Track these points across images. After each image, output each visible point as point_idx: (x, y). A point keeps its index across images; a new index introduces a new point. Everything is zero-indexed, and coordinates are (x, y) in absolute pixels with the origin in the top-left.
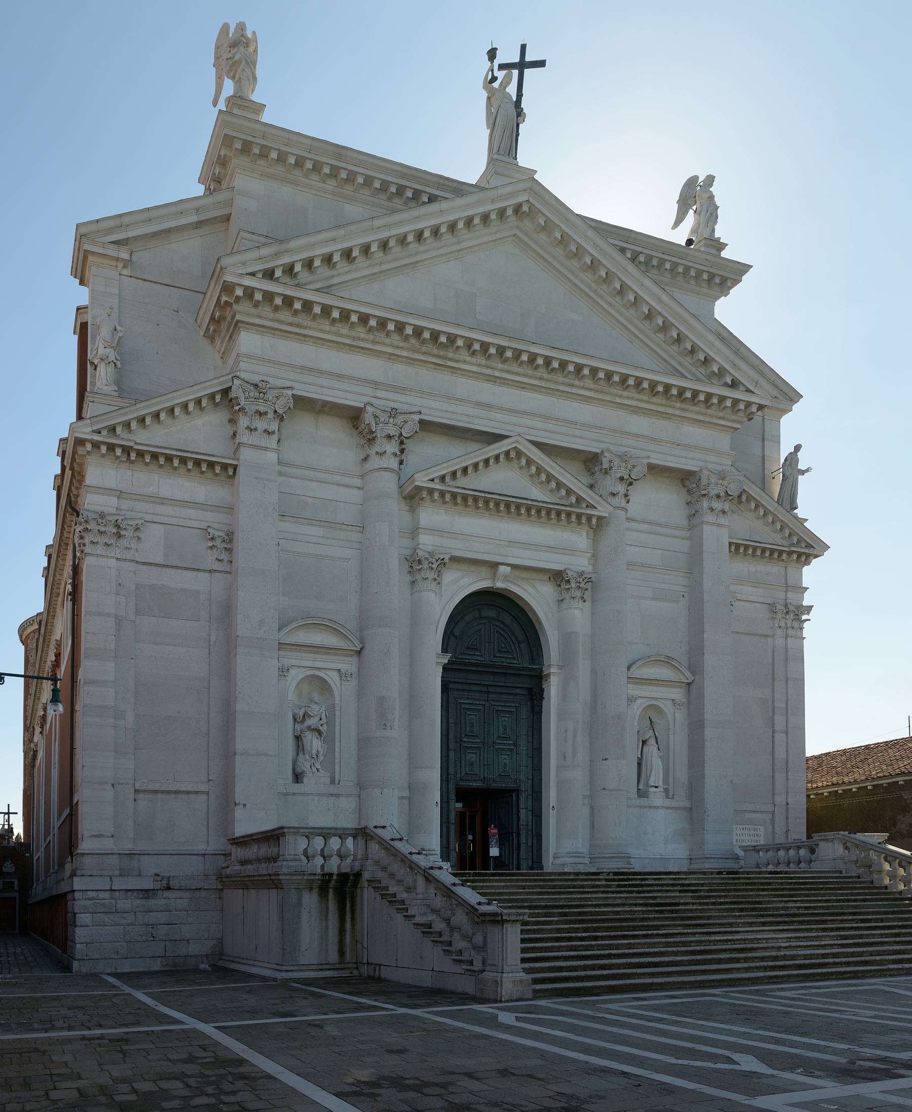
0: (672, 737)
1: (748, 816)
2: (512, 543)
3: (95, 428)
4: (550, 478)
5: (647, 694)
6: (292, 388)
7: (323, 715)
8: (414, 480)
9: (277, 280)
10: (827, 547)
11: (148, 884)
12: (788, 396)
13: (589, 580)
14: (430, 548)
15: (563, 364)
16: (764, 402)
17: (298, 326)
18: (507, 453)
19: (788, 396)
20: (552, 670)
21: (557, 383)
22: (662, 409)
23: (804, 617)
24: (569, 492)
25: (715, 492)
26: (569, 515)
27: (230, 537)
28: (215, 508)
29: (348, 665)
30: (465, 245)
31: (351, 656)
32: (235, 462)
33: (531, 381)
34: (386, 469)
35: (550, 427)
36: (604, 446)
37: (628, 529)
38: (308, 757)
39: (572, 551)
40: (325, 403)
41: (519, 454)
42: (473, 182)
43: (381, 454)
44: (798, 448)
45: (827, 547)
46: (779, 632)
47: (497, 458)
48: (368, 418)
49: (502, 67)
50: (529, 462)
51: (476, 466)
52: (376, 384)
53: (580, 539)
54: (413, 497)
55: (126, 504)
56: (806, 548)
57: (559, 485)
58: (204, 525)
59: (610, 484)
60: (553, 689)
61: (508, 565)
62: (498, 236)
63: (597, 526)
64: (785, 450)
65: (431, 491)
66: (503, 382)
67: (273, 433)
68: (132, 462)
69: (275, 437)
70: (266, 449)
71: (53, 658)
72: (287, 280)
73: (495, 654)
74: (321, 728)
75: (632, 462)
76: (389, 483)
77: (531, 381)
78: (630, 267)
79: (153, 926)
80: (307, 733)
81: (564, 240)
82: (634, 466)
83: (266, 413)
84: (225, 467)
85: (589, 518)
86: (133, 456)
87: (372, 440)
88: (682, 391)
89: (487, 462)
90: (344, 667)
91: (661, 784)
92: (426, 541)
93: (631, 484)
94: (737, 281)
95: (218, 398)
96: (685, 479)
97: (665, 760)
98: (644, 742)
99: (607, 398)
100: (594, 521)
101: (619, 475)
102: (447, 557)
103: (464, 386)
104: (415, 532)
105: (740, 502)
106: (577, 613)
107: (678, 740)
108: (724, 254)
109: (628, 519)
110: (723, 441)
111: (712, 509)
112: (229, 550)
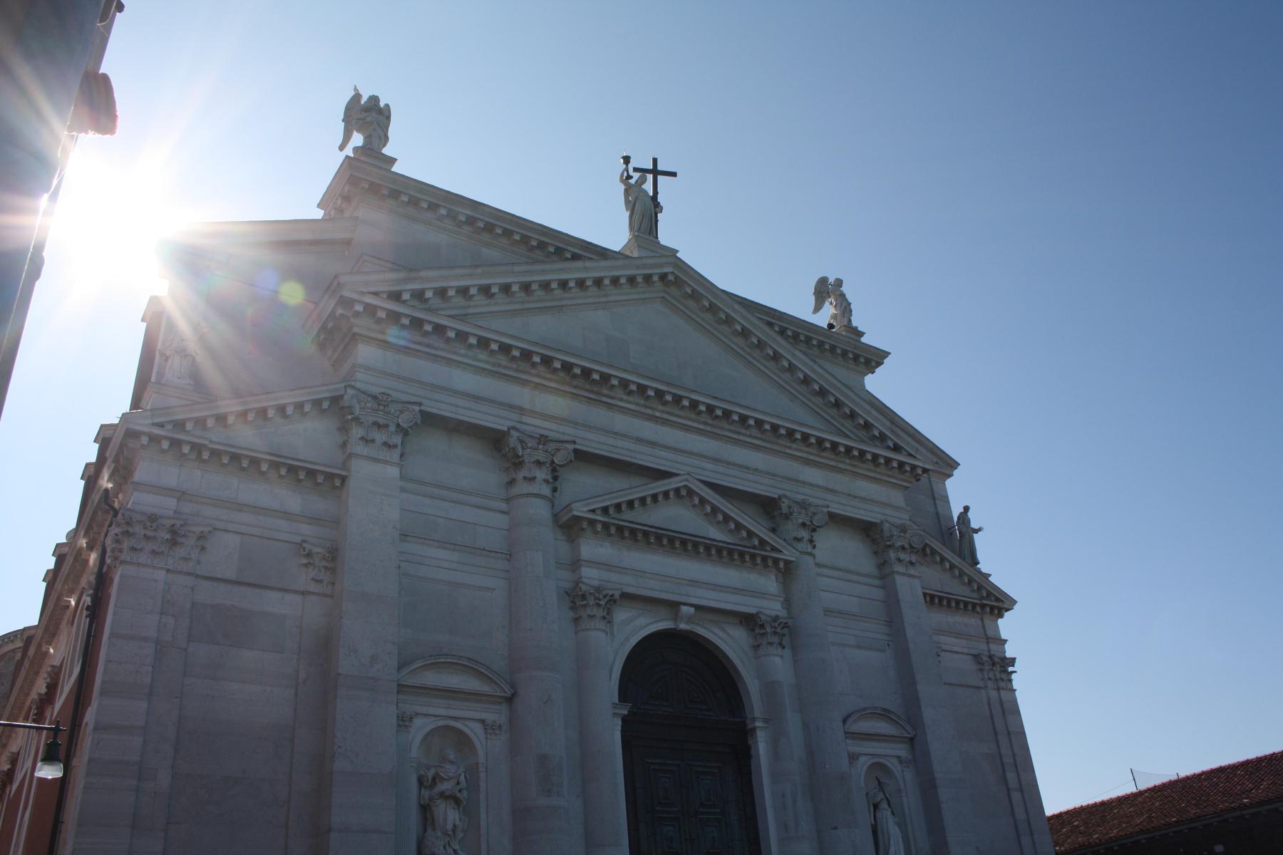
0: (905, 799)
2: (694, 583)
3: (156, 420)
4: (727, 518)
6: (420, 404)
7: (462, 777)
8: (571, 510)
9: (404, 302)
10: (1015, 602)
12: (947, 465)
13: (786, 626)
14: (596, 583)
15: (727, 414)
16: (927, 466)
17: (429, 346)
18: (677, 490)
19: (947, 465)
20: (757, 724)
21: (723, 429)
22: (832, 463)
23: (1010, 669)
24: (751, 534)
25: (899, 544)
26: (753, 556)
27: (334, 554)
28: (315, 520)
30: (611, 299)
31: (500, 703)
32: (344, 473)
33: (695, 425)
34: (537, 496)
35: (721, 469)
36: (781, 492)
37: (818, 575)
38: (439, 834)
39: (763, 595)
40: (461, 423)
41: (691, 493)
42: (617, 249)
43: (532, 479)
44: (966, 509)
45: (1015, 602)
46: (990, 684)
47: (666, 494)
48: (513, 441)
49: (636, 170)
50: (703, 501)
51: (643, 500)
54: (570, 527)
56: (998, 603)
57: (739, 526)
58: (298, 539)
59: (791, 529)
60: (762, 745)
61: (692, 605)
62: (646, 296)
63: (786, 571)
64: (956, 511)
65: (592, 522)
66: (665, 422)
67: (395, 446)
68: (205, 461)
69: (398, 451)
70: (386, 462)
71: (43, 690)
72: (416, 303)
74: (458, 795)
75: (812, 509)
76: (541, 510)
77: (695, 425)
78: (779, 338)
80: (438, 802)
81: (713, 309)
82: (815, 514)
83: (387, 426)
84: (330, 477)
85: (776, 561)
86: (206, 455)
87: (517, 463)
88: (849, 450)
89: (655, 497)
90: (489, 717)
92: (591, 576)
93: (814, 530)
94: (879, 364)
95: (325, 405)
96: (868, 530)
97: (902, 825)
98: (876, 806)
99: (776, 447)
100: (782, 565)
101: (800, 521)
103: (621, 422)
104: (575, 564)
105: (925, 555)
106: (777, 659)
107: (911, 801)
108: (863, 340)
109: (818, 565)
110: (897, 498)
111: (899, 560)
112: (333, 570)
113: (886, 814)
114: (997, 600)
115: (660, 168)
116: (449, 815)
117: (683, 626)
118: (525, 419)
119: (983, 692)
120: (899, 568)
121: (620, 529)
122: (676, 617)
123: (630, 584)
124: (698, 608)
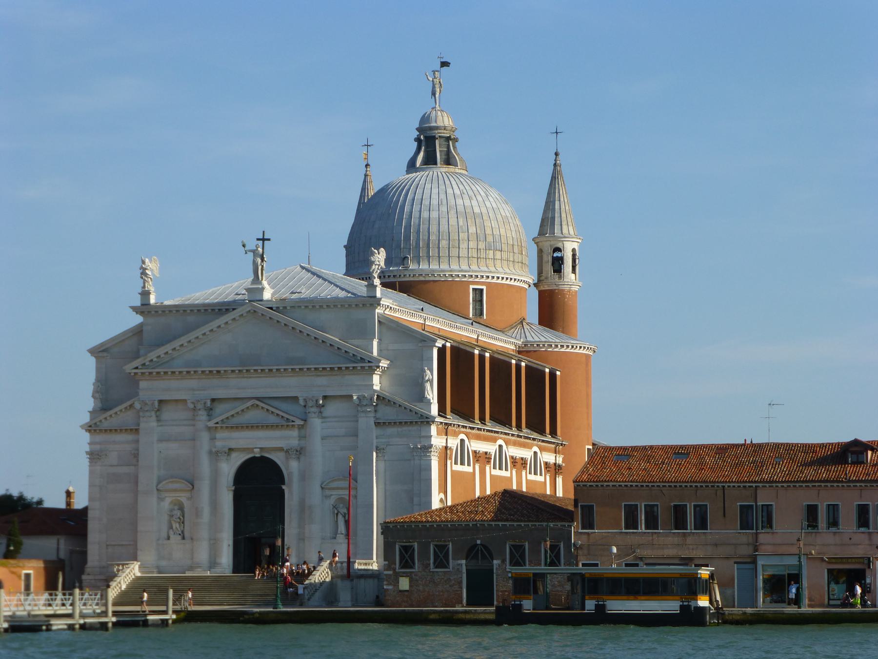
18: (252, 405)
29: (188, 494)
47: (248, 408)
53: (295, 433)
89: (243, 410)
92: (219, 444)
113: (340, 517)
116: (175, 525)
120: (363, 415)
121: (227, 427)
123: (233, 447)
124: (261, 448)
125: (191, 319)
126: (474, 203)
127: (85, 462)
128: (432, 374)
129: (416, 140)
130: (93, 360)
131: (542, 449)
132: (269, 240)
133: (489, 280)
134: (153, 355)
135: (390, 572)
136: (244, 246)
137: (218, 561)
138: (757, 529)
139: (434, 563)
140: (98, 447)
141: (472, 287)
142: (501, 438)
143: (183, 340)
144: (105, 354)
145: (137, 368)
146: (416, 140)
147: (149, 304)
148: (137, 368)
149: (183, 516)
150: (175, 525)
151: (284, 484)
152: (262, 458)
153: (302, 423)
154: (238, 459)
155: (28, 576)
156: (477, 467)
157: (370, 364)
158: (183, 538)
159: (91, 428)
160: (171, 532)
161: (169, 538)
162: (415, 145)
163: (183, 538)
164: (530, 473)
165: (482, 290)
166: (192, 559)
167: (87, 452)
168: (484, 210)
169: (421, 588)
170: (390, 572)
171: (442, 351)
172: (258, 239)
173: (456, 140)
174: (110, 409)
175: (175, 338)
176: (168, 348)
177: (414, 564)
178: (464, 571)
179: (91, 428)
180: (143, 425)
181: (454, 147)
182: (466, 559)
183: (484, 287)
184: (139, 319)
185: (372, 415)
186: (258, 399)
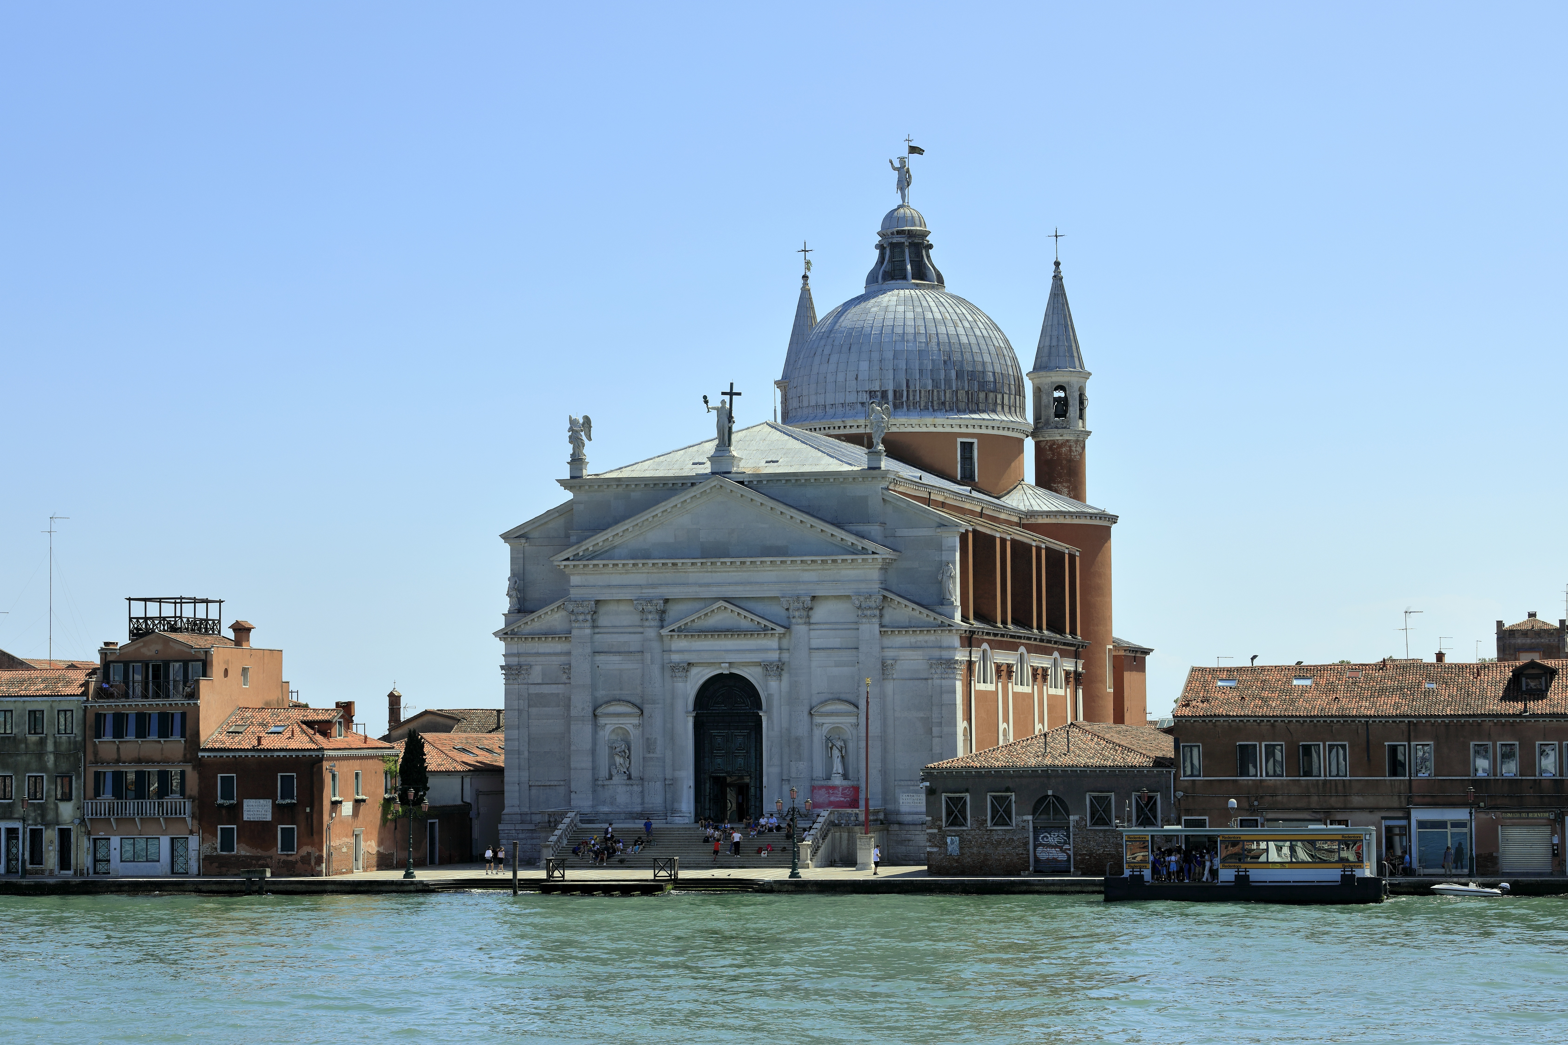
1: (912, 788)
5: (831, 721)
11: (532, 827)
29: (636, 721)
52: (640, 586)
55: (522, 659)
73: (728, 709)
79: (535, 845)
91: (840, 771)
92: (676, 658)
102: (685, 665)
114: (949, 625)
115: (734, 391)
117: (726, 672)
118: (644, 591)
119: (930, 681)
122: (721, 668)
125: (636, 495)
126: (961, 331)
127: (500, 679)
128: (955, 569)
129: (877, 247)
130: (507, 548)
131: (1063, 654)
132: (739, 394)
133: (983, 431)
134: (589, 545)
135: (936, 831)
136: (706, 402)
137: (676, 805)
138: (1410, 776)
139: (993, 818)
140: (514, 660)
141: (959, 440)
142: (1023, 644)
143: (628, 524)
144: (523, 541)
145: (568, 559)
146: (877, 247)
147: (581, 477)
148: (568, 559)
149: (629, 749)
150: (619, 760)
151: (761, 709)
152: (732, 675)
153: (782, 630)
154: (700, 676)
155: (432, 824)
156: (1000, 685)
157: (875, 556)
158: (630, 778)
159: (504, 635)
160: (614, 772)
161: (611, 777)
162: (876, 253)
163: (630, 778)
164: (1051, 687)
165: (972, 443)
166: (643, 803)
167: (502, 667)
168: (973, 340)
169: (975, 850)
170: (936, 831)
171: (964, 537)
172: (723, 393)
173: (930, 246)
174: (533, 612)
175: (617, 521)
176: (609, 534)
177: (965, 819)
178: (1031, 829)
179: (504, 635)
180: (575, 632)
181: (928, 257)
182: (1033, 814)
183: (975, 441)
184: (568, 496)
185: (876, 620)
186: (727, 600)
